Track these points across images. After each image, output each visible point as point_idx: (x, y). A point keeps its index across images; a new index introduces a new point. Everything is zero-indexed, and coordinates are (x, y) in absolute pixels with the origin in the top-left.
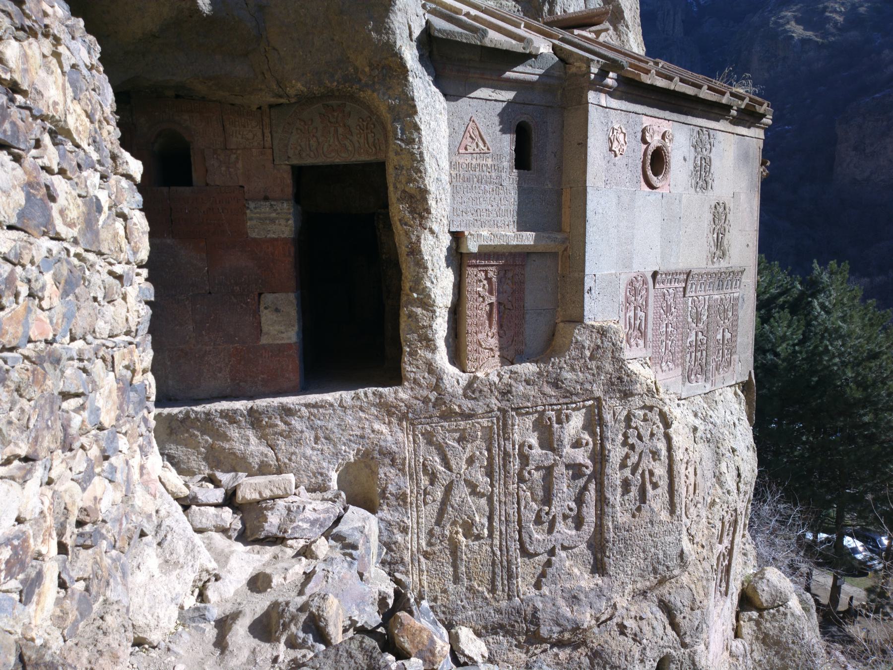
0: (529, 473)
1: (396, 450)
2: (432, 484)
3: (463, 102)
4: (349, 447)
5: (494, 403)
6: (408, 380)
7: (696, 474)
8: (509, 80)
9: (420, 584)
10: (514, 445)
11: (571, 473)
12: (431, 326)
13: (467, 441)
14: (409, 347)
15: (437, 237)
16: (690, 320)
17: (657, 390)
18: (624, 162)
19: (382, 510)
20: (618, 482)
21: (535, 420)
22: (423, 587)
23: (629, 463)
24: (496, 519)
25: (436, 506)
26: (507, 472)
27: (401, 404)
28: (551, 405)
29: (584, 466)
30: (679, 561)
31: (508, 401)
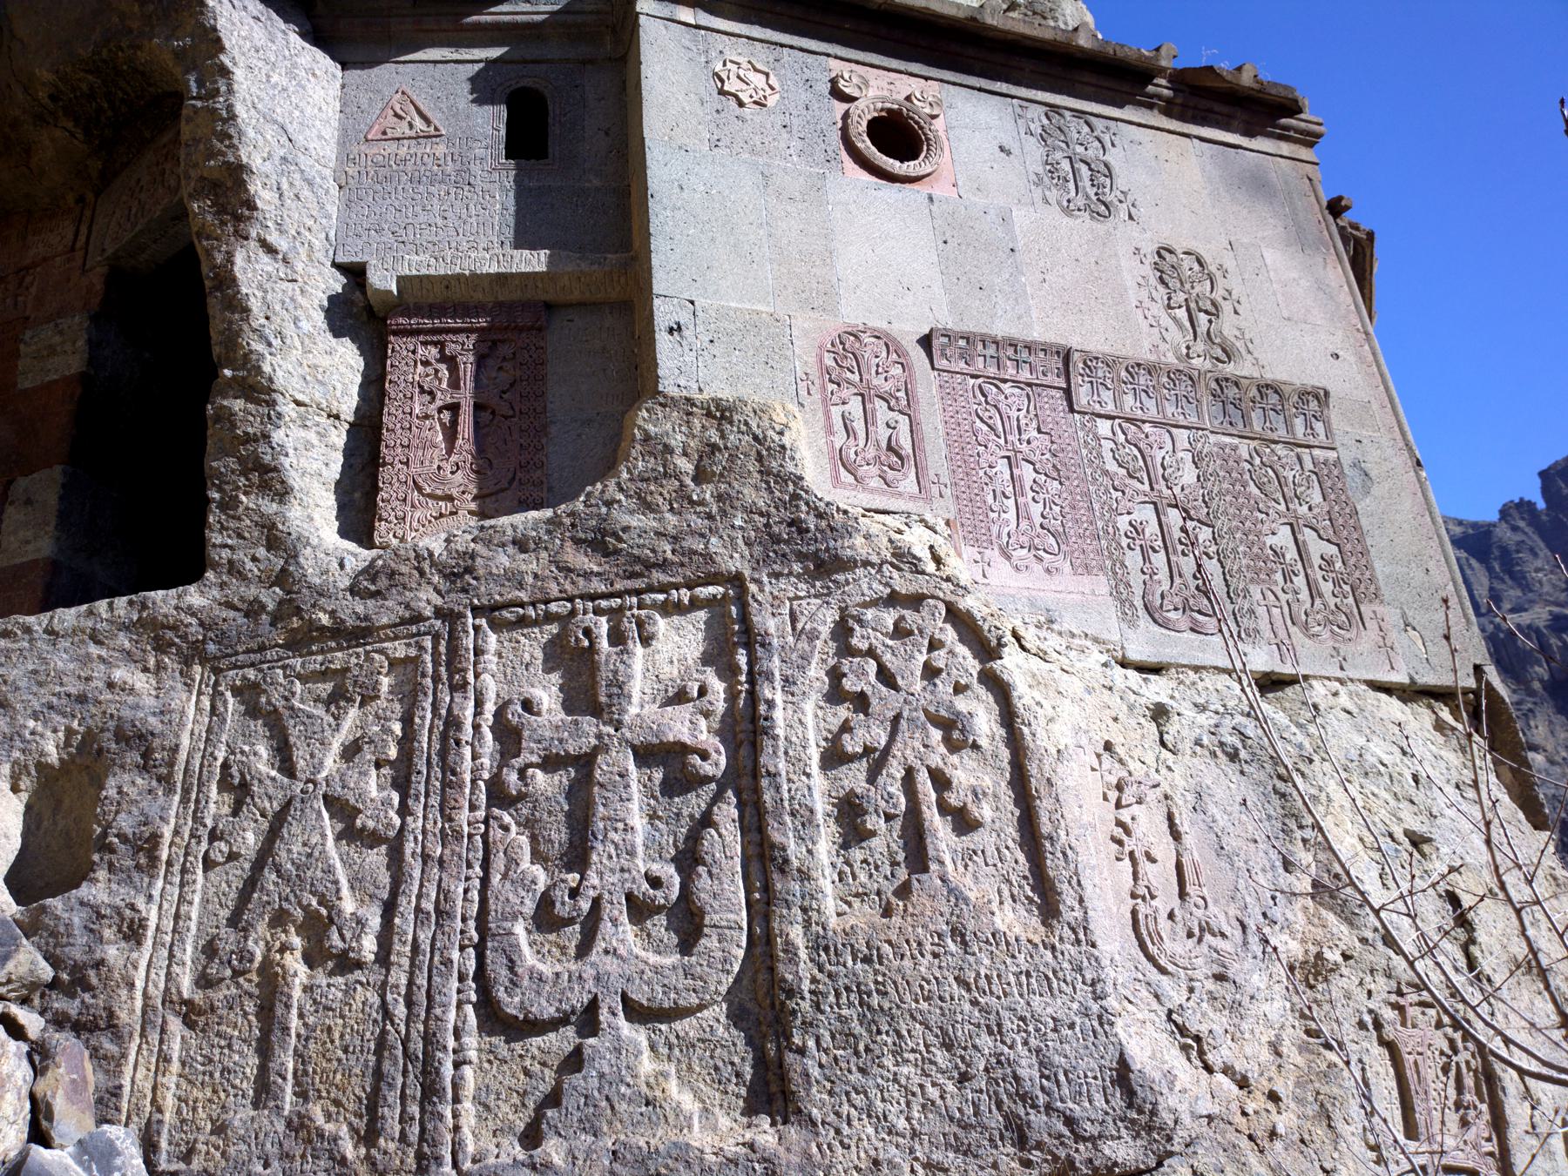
0: (522, 773)
2: (235, 812)
3: (384, 72)
6: (215, 566)
7: (1176, 835)
8: (478, 27)
10: (479, 704)
11: (658, 775)
12: (266, 437)
13: (350, 700)
14: (220, 490)
15: (285, 260)
16: (1112, 466)
17: (938, 560)
18: (779, 120)
20: (821, 806)
21: (550, 641)
24: (406, 905)
25: (237, 874)
26: (449, 769)
27: (189, 620)
29: (696, 751)
30: (1118, 1101)
31: (465, 590)
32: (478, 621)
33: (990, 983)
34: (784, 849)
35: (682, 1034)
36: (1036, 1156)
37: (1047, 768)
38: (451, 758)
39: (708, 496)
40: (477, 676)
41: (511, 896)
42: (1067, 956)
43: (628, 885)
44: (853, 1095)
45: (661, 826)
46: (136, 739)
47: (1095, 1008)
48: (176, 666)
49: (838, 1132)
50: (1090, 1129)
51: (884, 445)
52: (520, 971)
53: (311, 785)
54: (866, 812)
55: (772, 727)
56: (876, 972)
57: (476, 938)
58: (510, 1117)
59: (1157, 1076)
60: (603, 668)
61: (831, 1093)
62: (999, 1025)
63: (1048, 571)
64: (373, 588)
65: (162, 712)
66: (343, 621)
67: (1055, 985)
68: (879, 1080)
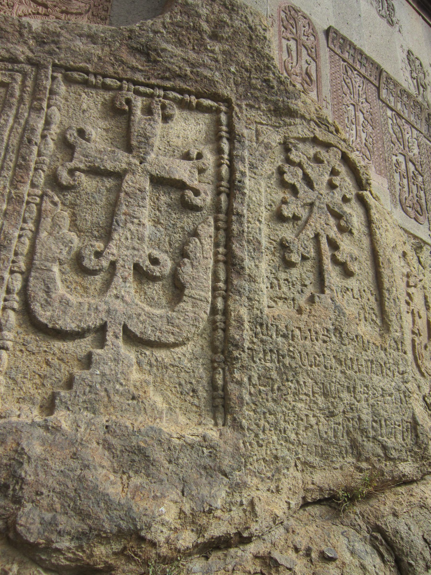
0: (71, 172)
10: (48, 123)
32: (55, 74)
33: (352, 362)
34: (242, 261)
35: (160, 359)
36: (364, 465)
37: (387, 253)
38: (23, 151)
40: (49, 106)
41: (53, 247)
42: (392, 356)
43: (136, 259)
44: (267, 415)
45: (162, 229)
47: (403, 387)
49: (257, 435)
50: (395, 454)
51: (304, 69)
52: (53, 296)
54: (292, 252)
55: (244, 188)
56: (290, 345)
57: (23, 267)
58: (32, 391)
60: (136, 125)
61: (255, 411)
62: (354, 388)
67: (384, 371)
68: (284, 409)
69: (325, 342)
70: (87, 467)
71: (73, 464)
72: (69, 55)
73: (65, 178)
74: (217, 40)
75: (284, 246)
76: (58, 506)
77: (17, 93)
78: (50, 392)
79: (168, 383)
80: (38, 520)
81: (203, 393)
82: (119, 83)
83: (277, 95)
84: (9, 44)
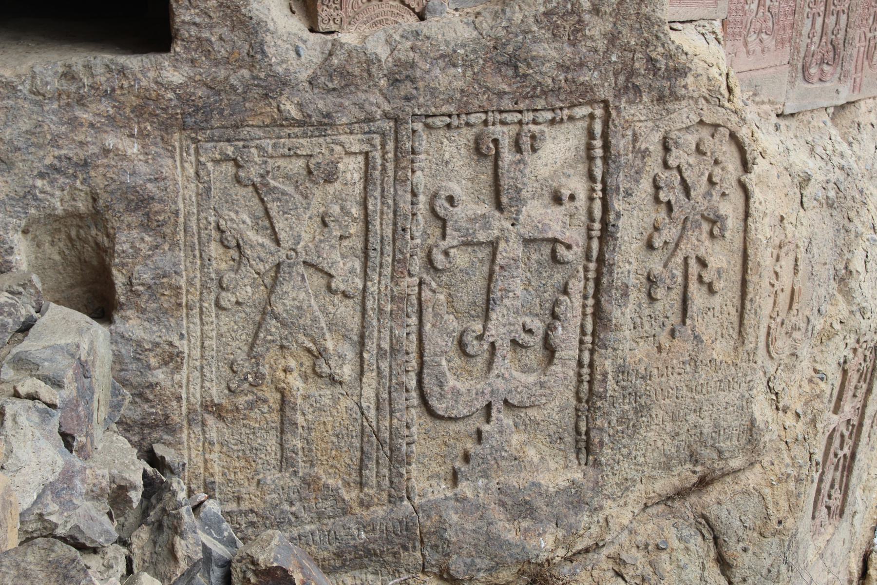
0: (446, 253)
1: (158, 194)
4: (52, 182)
5: (376, 101)
9: (206, 469)
10: (414, 194)
17: (730, 90)
19: (126, 319)
22: (212, 475)
23: (658, 243)
24: (371, 345)
28: (501, 112)
31: (407, 99)
35: (533, 418)
37: (759, 254)
39: (597, 33)
40: (413, 172)
43: (513, 334)
46: (140, 202)
47: (747, 395)
48: (156, 133)
49: (612, 468)
52: (446, 389)
53: (293, 253)
59: (762, 426)
61: (612, 449)
63: (763, 51)
64: (330, 85)
65: (156, 179)
66: (310, 116)
69: (679, 374)
70: (491, 523)
71: (480, 523)
72: (428, 97)
73: (439, 259)
74: (598, 15)
75: (651, 281)
76: (474, 553)
77: (379, 161)
78: (450, 467)
79: (539, 436)
80: (462, 564)
81: (569, 439)
82: (483, 116)
83: (663, 78)
84: (359, 94)
